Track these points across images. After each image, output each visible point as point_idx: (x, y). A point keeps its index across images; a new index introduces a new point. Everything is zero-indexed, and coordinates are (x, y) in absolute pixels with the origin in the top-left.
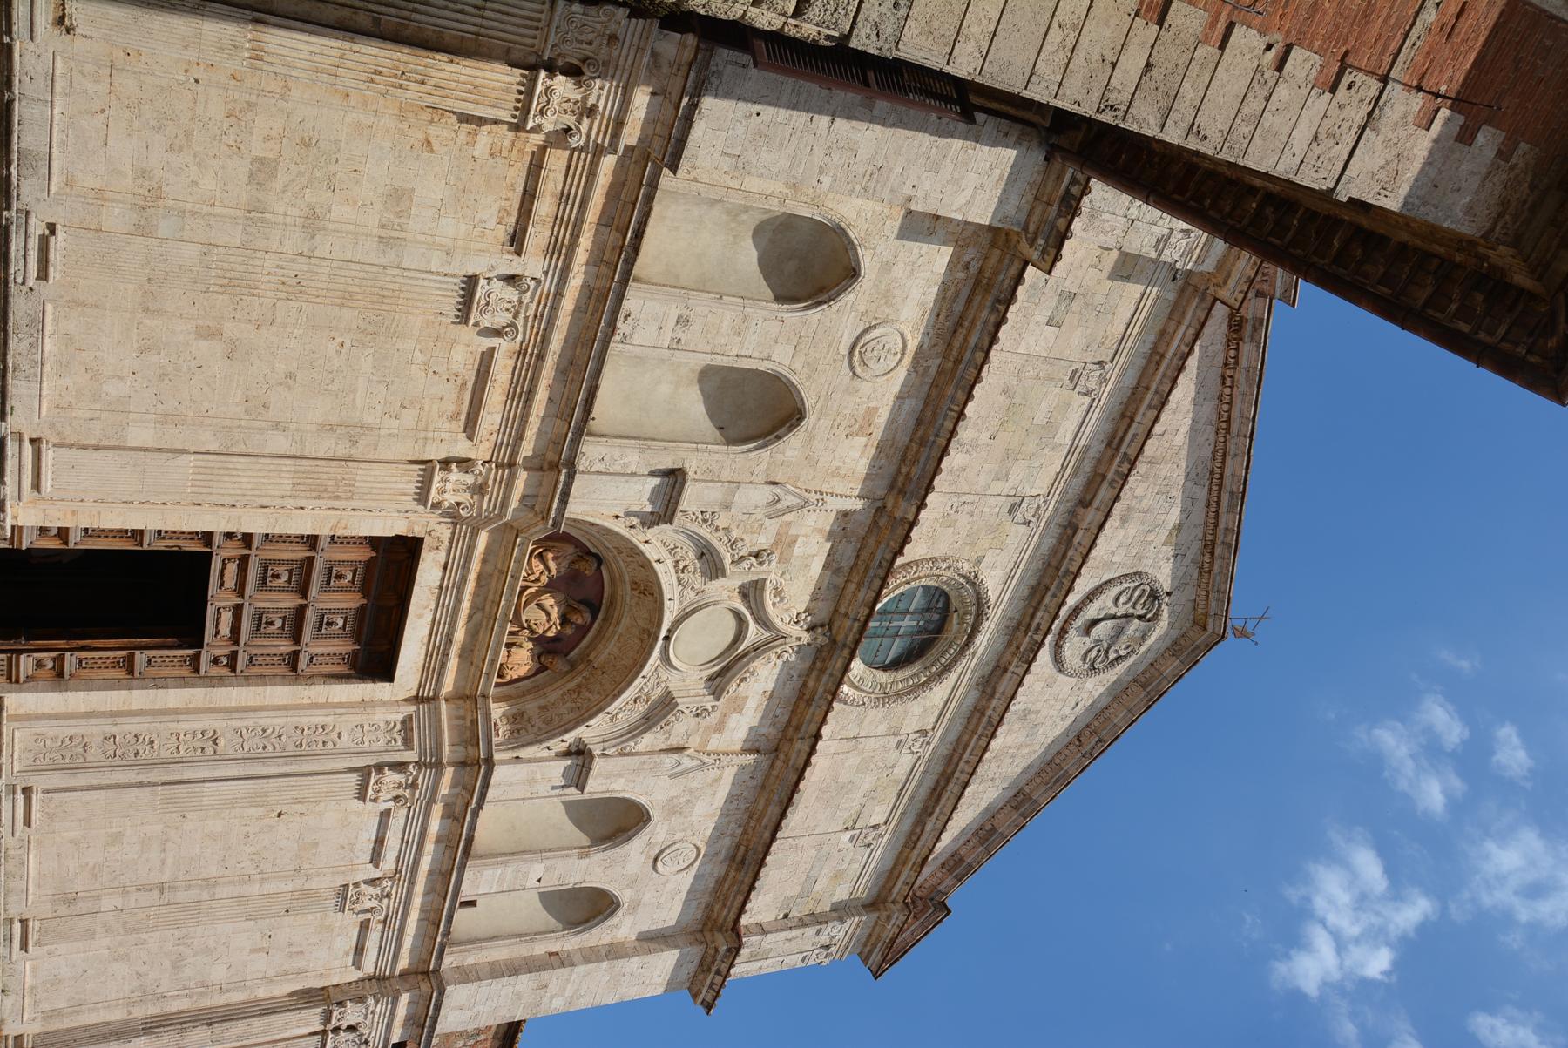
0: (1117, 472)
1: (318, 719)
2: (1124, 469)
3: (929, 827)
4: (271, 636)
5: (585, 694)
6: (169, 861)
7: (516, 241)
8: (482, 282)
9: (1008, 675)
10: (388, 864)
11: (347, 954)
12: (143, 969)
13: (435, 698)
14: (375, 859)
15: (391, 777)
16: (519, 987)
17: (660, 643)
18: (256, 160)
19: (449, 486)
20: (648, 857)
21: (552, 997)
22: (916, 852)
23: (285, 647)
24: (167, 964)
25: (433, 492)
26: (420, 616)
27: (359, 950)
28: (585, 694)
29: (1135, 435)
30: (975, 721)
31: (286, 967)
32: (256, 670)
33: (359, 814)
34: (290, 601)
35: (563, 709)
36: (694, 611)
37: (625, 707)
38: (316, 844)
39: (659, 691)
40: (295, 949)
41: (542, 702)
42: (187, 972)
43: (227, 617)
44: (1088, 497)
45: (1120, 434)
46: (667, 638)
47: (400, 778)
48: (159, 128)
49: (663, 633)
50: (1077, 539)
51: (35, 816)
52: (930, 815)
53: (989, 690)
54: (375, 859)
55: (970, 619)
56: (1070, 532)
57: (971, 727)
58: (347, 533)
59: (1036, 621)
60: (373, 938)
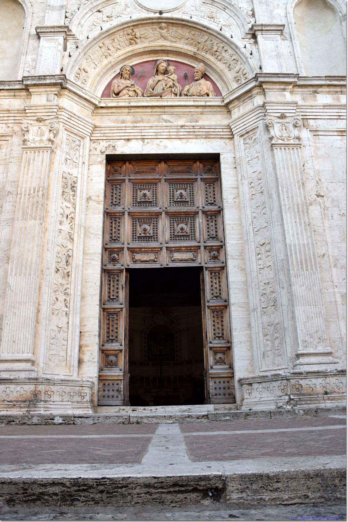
1: (245, 189)
4: (193, 229)
5: (215, 48)
13: (229, 127)
15: (276, 131)
19: (37, 139)
23: (200, 221)
25: (42, 145)
26: (166, 147)
28: (215, 48)
32: (220, 234)
33: (317, 148)
34: (164, 223)
35: (226, 56)
36: (140, 5)
37: (221, 22)
39: (203, 9)
41: (226, 70)
43: (177, 256)
47: (277, 127)
49: (158, 15)
51: (320, 349)
58: (102, 195)
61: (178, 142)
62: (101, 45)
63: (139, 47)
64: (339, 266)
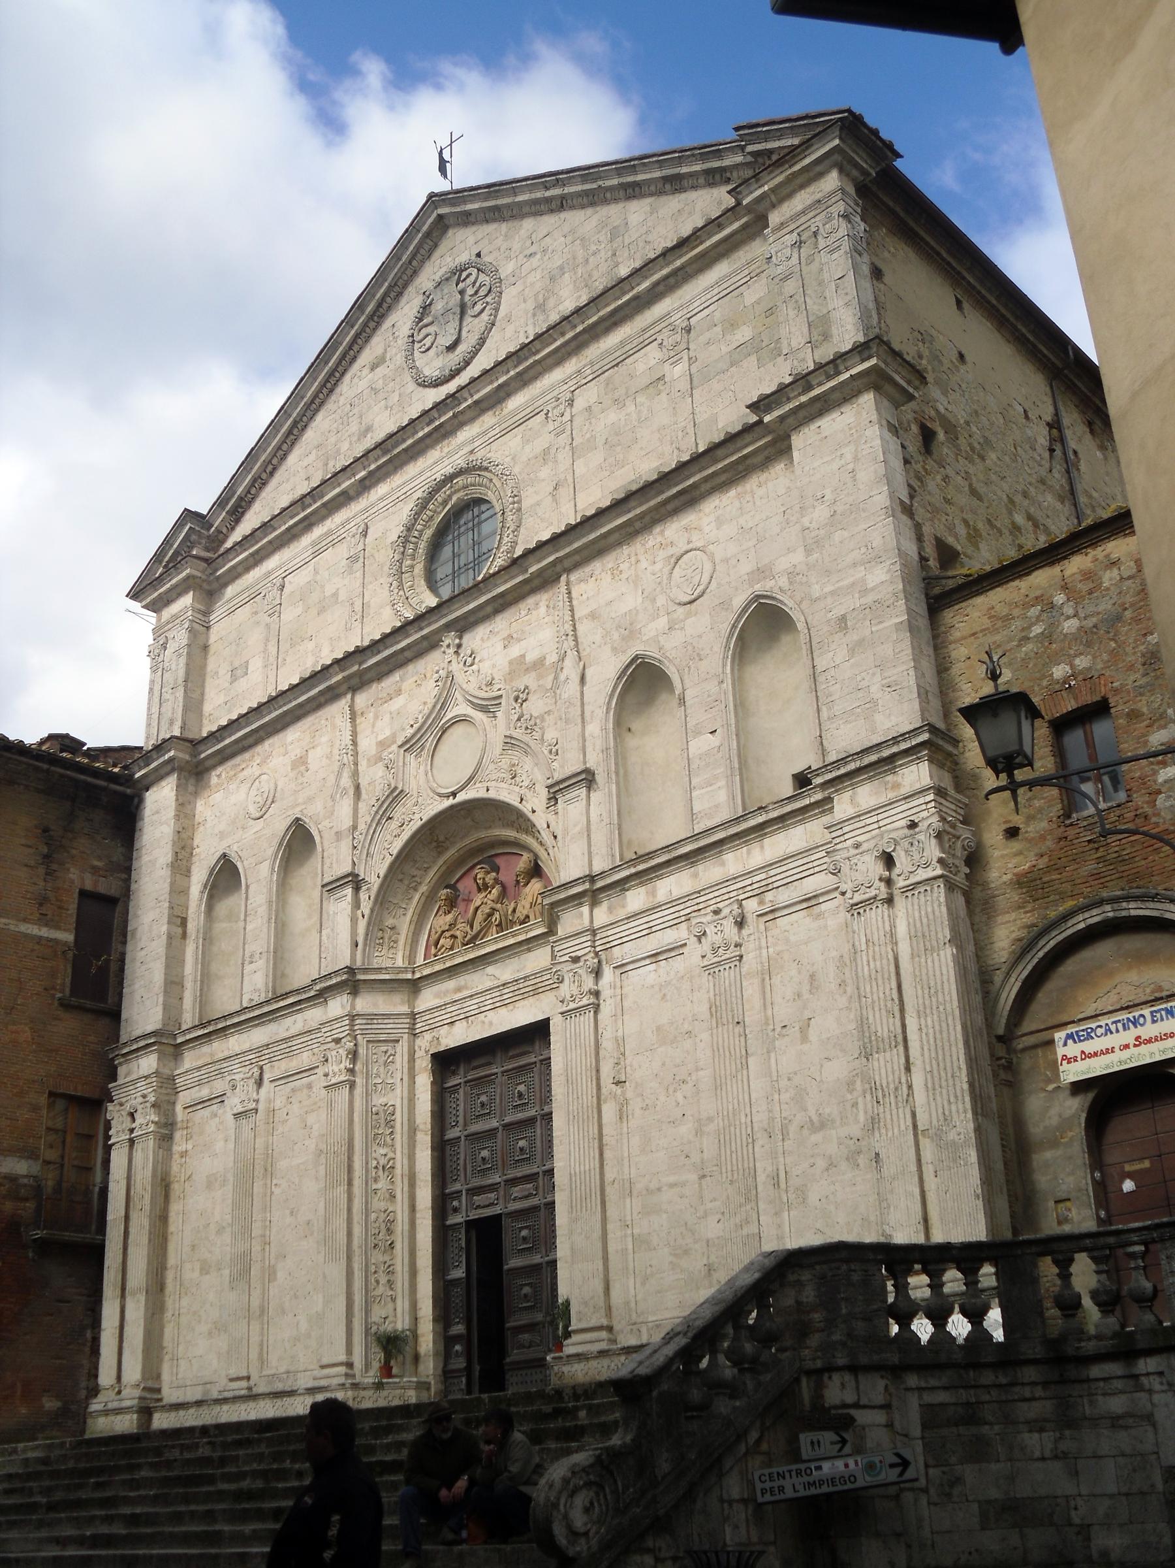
0: (315, 502)
2: (308, 500)
3: (646, 284)
6: (672, 1179)
7: (220, 1099)
8: (235, 1111)
9: (476, 397)
10: (681, 933)
11: (819, 916)
12: (821, 1163)
14: (676, 949)
16: (841, 654)
17: (461, 797)
18: (201, 1274)
20: (689, 615)
21: (864, 592)
22: (678, 263)
24: (815, 1138)
27: (810, 901)
29: (292, 518)
30: (531, 373)
31: (833, 986)
38: (658, 1028)
40: (806, 987)
42: (831, 1110)
44: (342, 498)
45: (301, 526)
46: (454, 794)
48: (193, 1330)
49: (451, 801)
50: (363, 473)
52: (636, 298)
53: (502, 394)
54: (676, 949)
55: (440, 497)
56: (367, 482)
57: (539, 368)
59: (427, 430)
60: (784, 896)
61: (503, 1011)
62: (400, 877)
63: (451, 853)
64: (635, 1193)
